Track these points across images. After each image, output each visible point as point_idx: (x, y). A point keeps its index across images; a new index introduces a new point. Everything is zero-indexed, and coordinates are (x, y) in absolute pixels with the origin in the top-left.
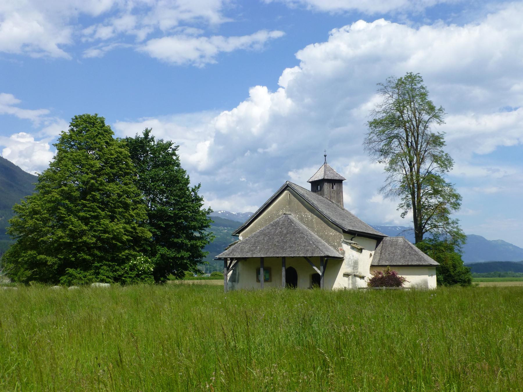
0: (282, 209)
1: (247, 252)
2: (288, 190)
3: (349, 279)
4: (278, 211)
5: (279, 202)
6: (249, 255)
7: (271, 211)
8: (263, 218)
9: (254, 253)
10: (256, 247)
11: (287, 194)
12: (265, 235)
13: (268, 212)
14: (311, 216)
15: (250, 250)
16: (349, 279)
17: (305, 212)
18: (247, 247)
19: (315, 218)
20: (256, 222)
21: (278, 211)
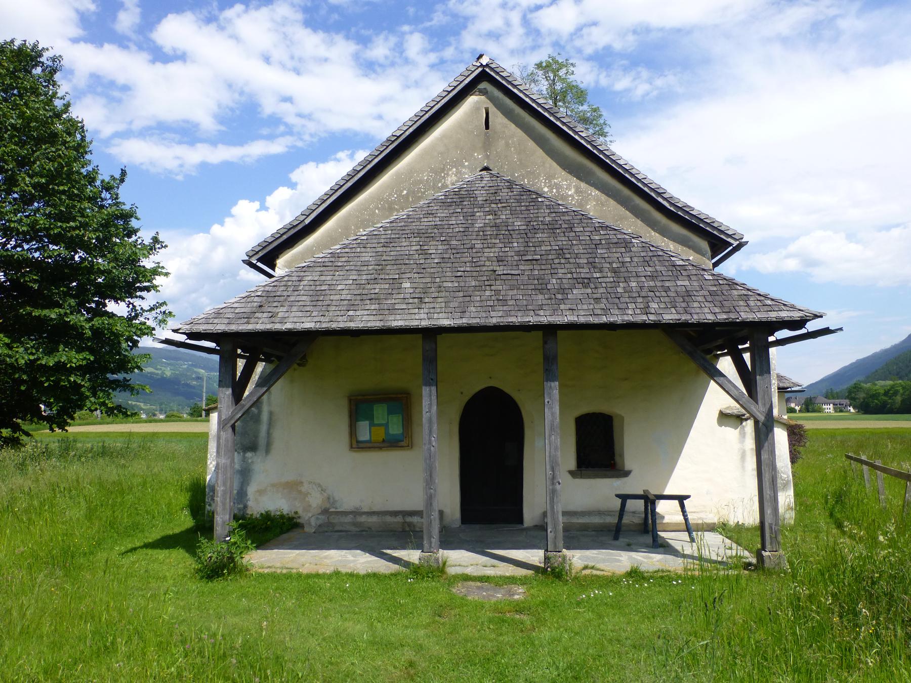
0: (458, 164)
1: (352, 306)
2: (484, 92)
3: (743, 435)
4: (440, 171)
5: (443, 137)
6: (364, 319)
7: (411, 171)
8: (377, 198)
9: (392, 310)
10: (396, 284)
11: (476, 108)
12: (424, 235)
13: (398, 175)
14: (578, 191)
15: (361, 298)
16: (743, 435)
17: (550, 177)
18: (344, 287)
19: (597, 200)
20: (349, 214)
21: (440, 171)
